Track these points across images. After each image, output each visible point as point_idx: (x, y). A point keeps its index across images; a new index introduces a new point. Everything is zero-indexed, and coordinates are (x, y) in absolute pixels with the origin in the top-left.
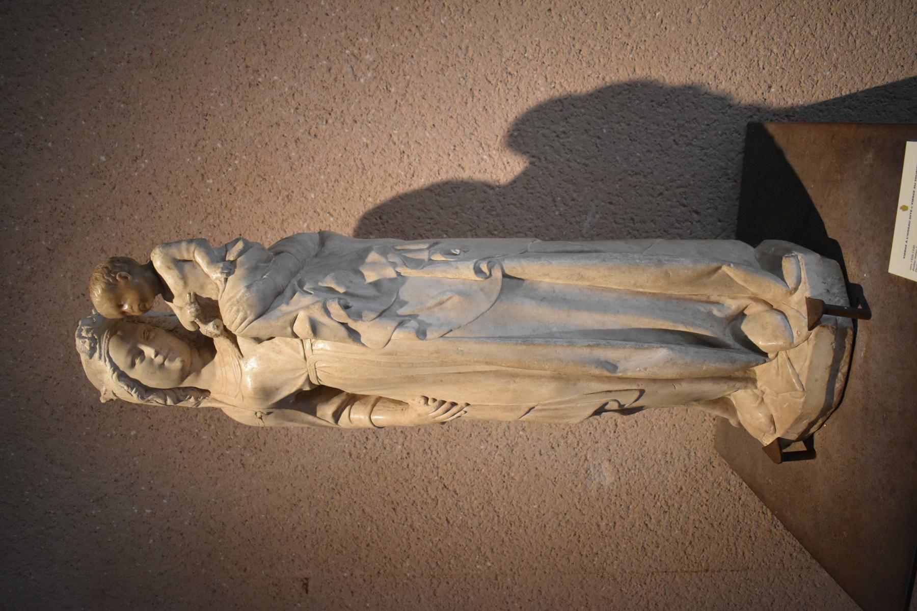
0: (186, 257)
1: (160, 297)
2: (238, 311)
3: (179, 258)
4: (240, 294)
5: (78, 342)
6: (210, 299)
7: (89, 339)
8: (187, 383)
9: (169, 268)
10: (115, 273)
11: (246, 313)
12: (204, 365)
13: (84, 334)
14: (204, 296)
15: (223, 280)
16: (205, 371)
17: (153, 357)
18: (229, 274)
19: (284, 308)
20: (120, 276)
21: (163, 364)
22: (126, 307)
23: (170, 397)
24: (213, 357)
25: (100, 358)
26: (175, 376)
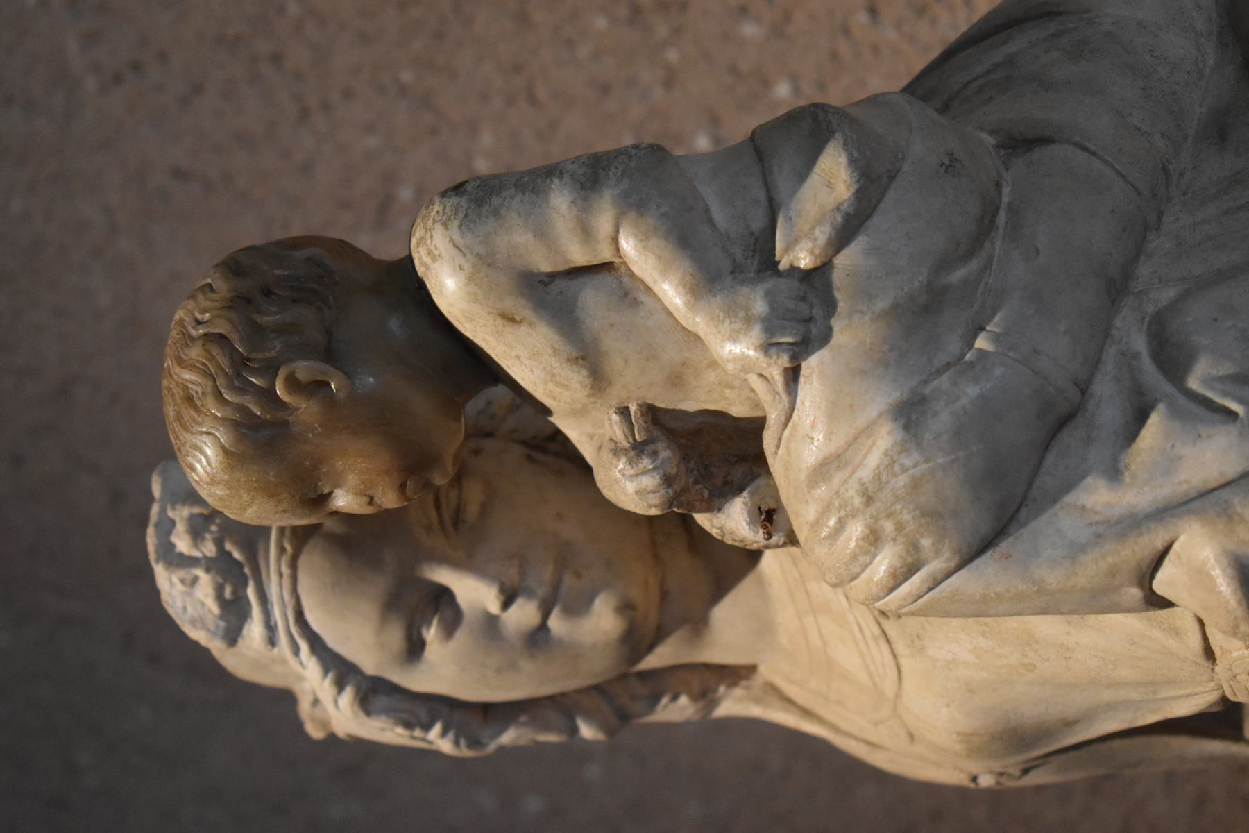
0: (578, 256)
2: (874, 539)
3: (546, 267)
4: (874, 459)
5: (168, 582)
7: (210, 565)
8: (652, 661)
9: (510, 319)
10: (270, 369)
11: (914, 547)
13: (182, 544)
14: (691, 406)
15: (776, 375)
17: (494, 607)
18: (801, 350)
19: (1097, 496)
20: (293, 384)
21: (543, 627)
22: (343, 500)
23: (590, 717)
25: (272, 641)
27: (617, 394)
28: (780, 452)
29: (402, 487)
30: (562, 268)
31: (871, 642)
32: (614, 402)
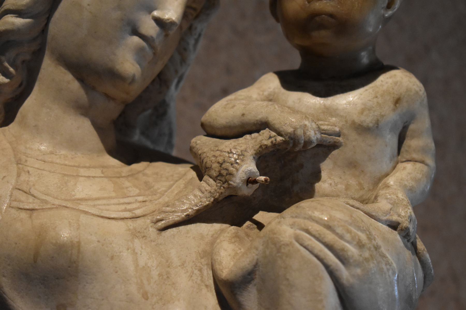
1: (295, 61)
6: (317, 176)
11: (358, 264)
12: (99, 129)
14: (326, 167)
15: (395, 218)
16: (84, 128)
17: (156, 13)
21: (135, 32)
23: (29, 27)
24: (113, 153)
26: (96, 53)
27: (353, 135)
28: (348, 206)
29: (331, 15)
30: (409, 133)
31: (123, 207)
32: (345, 131)
